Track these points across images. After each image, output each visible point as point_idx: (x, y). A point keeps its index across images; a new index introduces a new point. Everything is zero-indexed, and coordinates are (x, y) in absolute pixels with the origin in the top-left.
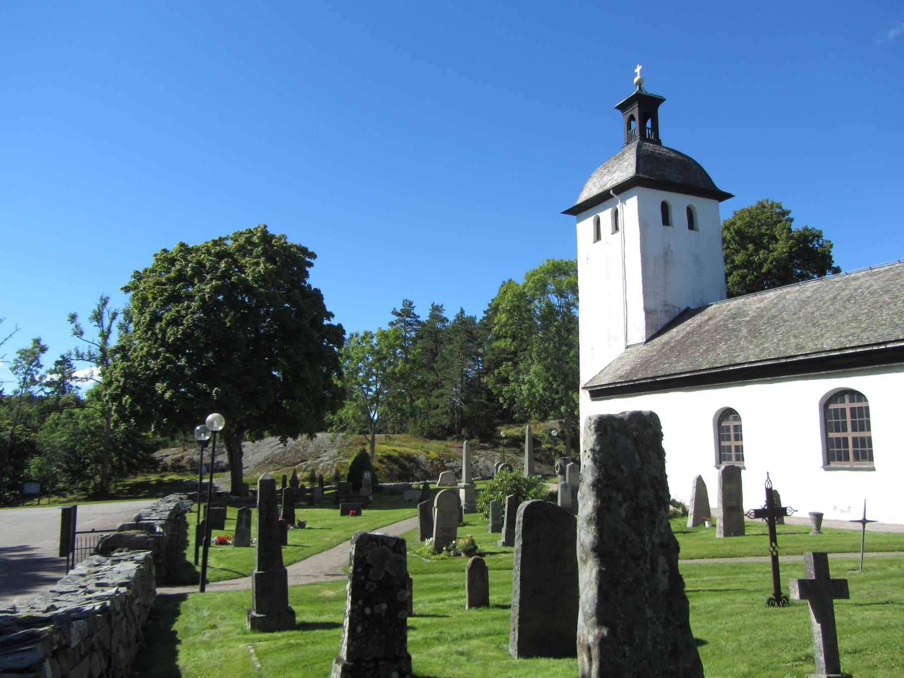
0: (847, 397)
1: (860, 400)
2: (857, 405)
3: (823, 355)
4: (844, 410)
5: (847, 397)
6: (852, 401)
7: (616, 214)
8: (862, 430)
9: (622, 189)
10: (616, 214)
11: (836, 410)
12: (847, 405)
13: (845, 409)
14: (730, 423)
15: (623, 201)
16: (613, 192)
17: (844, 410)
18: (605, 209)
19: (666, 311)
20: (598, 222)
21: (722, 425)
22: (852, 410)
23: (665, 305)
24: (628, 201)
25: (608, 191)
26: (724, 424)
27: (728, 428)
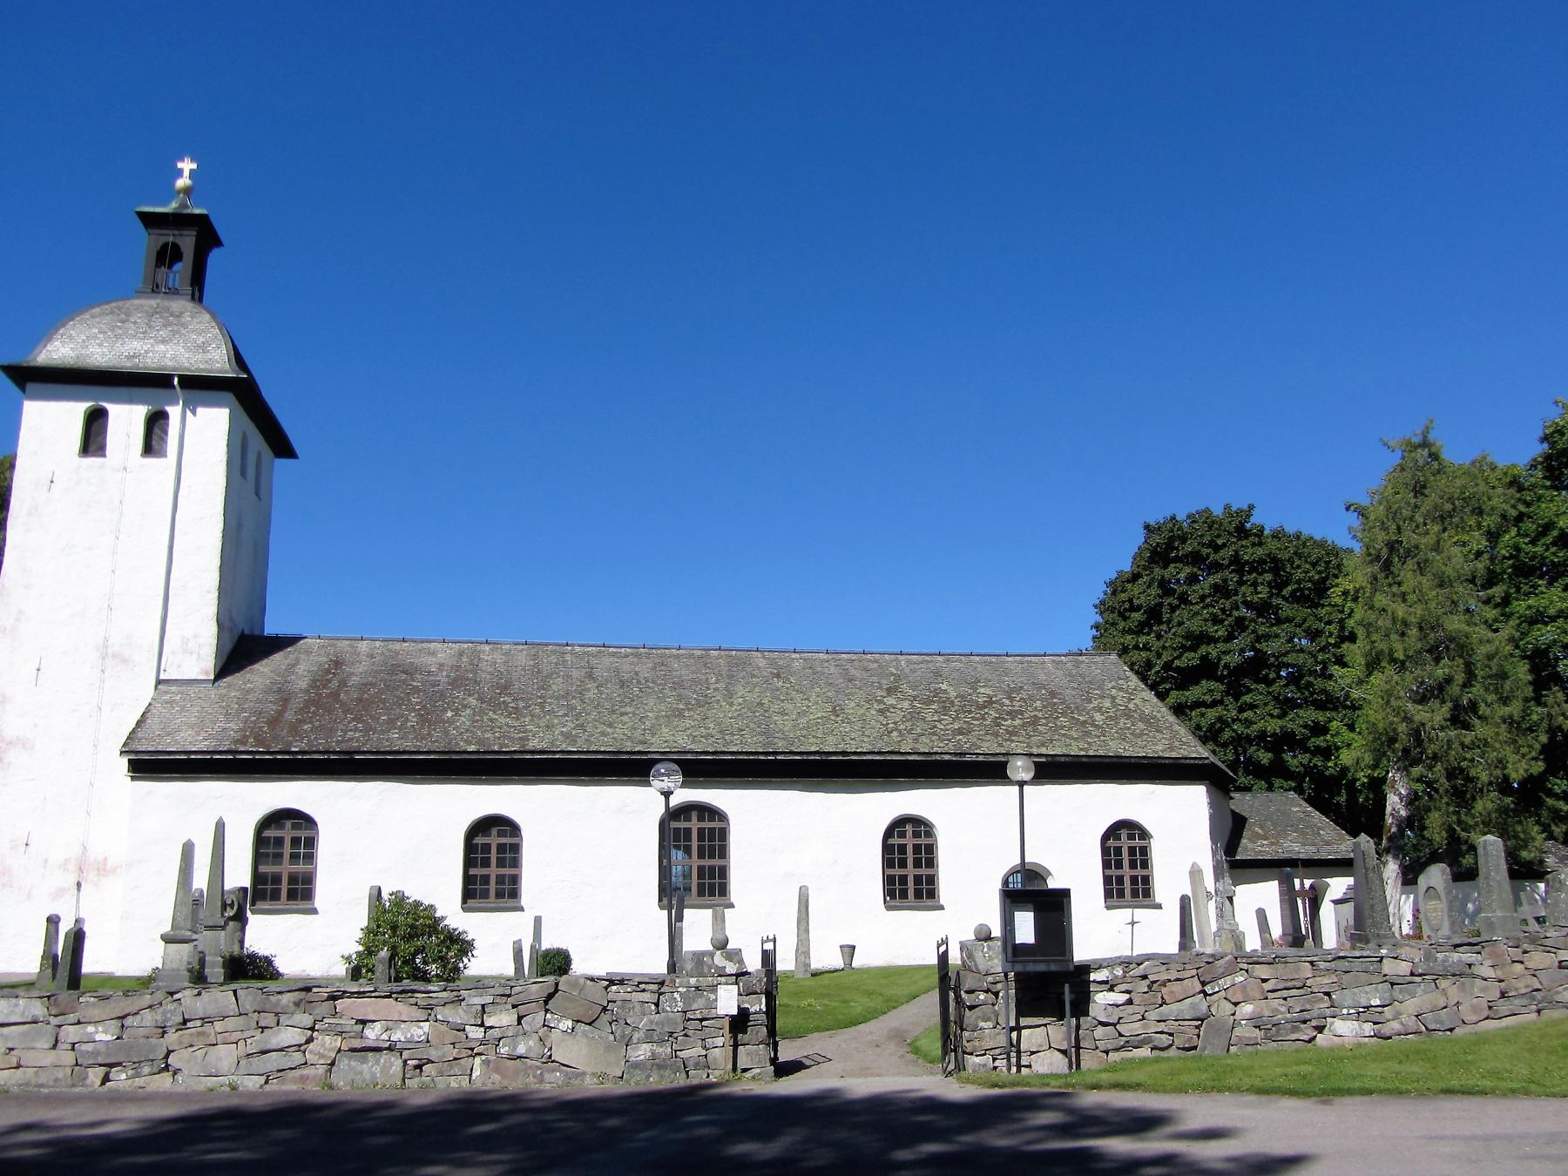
0: (694, 815)
1: (712, 819)
2: (707, 825)
3: (689, 757)
4: (688, 831)
5: (694, 815)
6: (701, 819)
7: (155, 423)
8: (712, 856)
9: (199, 386)
10: (156, 422)
11: (677, 830)
12: (694, 824)
13: (691, 829)
14: (494, 840)
15: (191, 406)
16: (179, 382)
17: (688, 831)
18: (130, 401)
19: (231, 630)
20: (95, 423)
21: (475, 842)
22: (701, 831)
23: (231, 619)
24: (200, 410)
25: (171, 377)
26: (479, 840)
27: (486, 848)
